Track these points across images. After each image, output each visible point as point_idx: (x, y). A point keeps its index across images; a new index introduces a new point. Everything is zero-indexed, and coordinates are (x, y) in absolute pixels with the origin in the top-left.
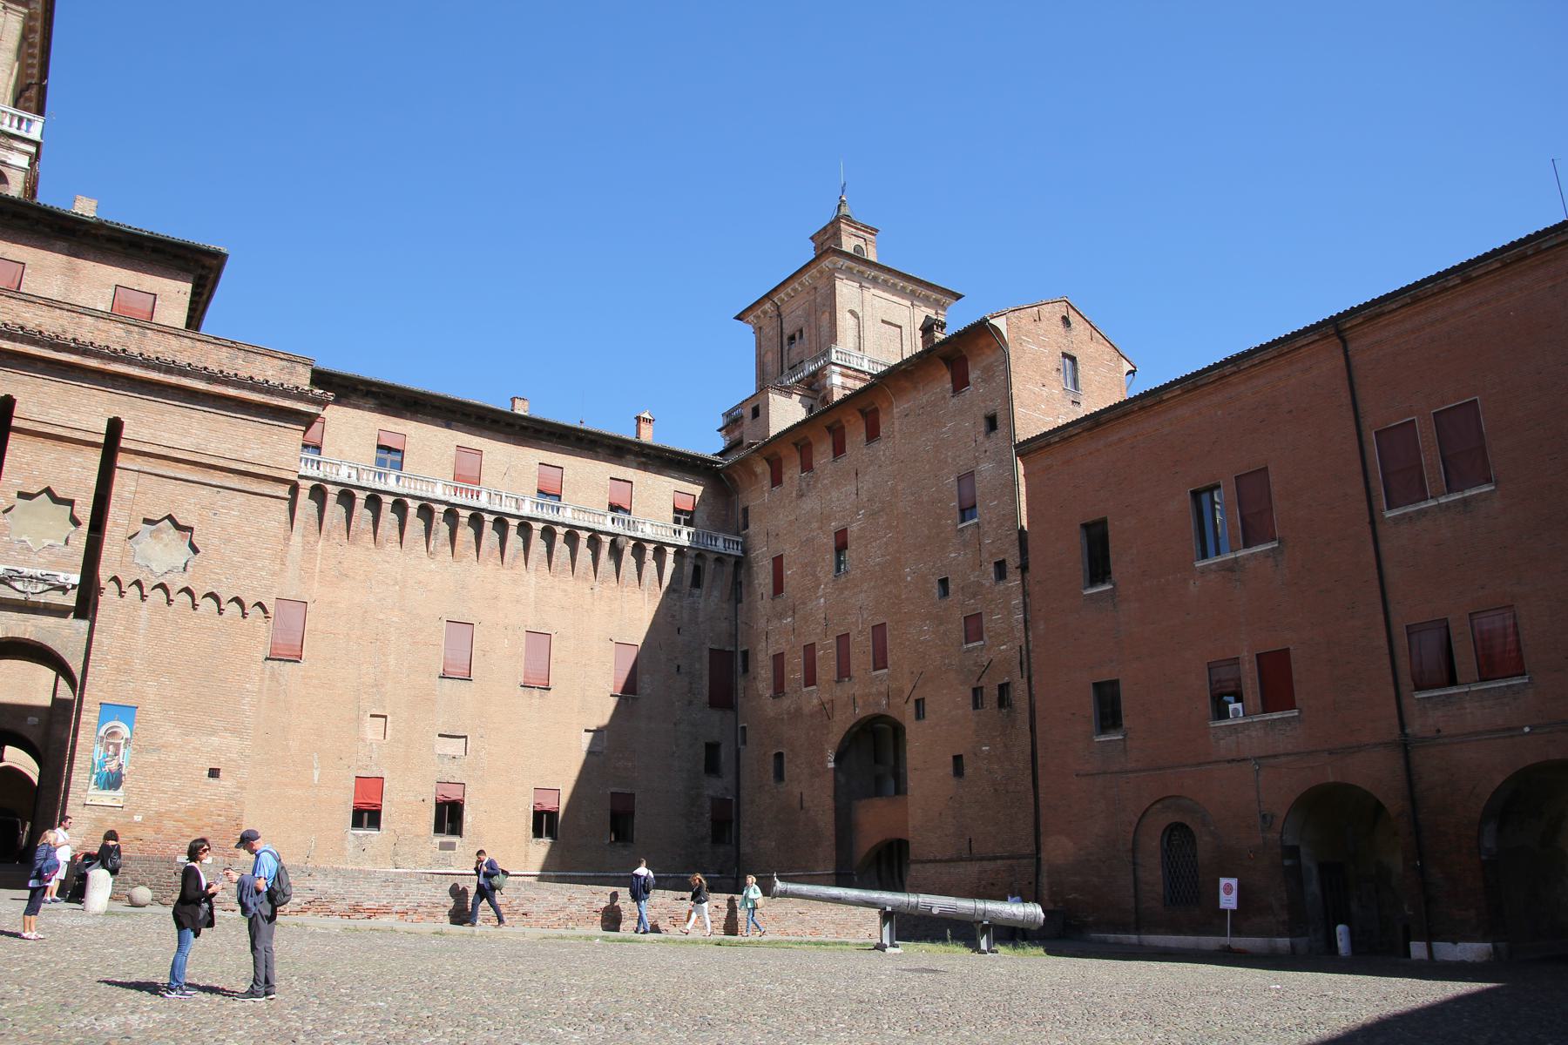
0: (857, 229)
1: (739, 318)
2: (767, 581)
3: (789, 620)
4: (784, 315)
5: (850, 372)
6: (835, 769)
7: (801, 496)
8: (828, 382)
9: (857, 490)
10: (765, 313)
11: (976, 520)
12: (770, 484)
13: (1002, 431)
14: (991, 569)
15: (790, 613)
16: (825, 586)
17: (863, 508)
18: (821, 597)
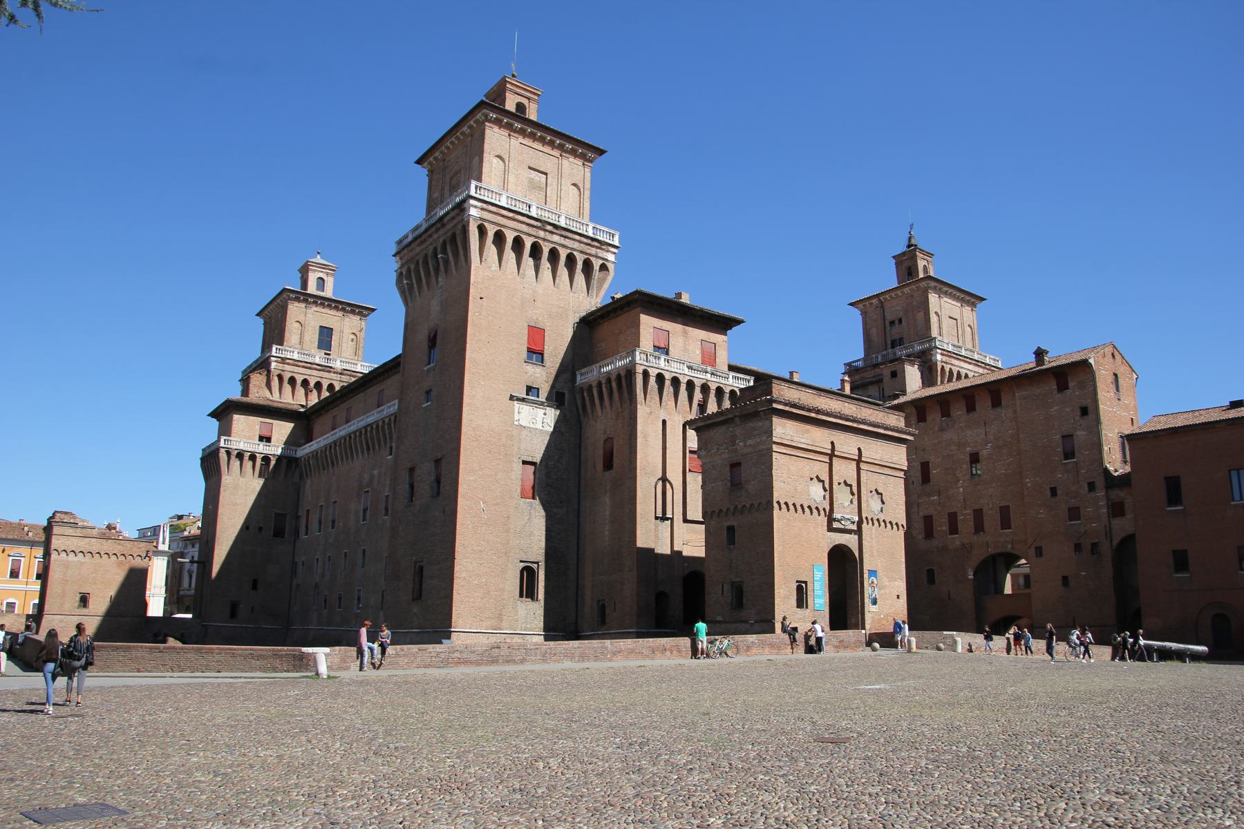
0: (923, 254)
1: (851, 304)
2: (917, 475)
3: (936, 497)
4: (885, 307)
5: (945, 352)
6: (974, 580)
7: (942, 430)
8: (933, 358)
9: (986, 432)
10: (871, 304)
11: (1075, 460)
12: (916, 421)
13: (1091, 416)
14: (1086, 485)
15: (936, 494)
16: (964, 481)
17: (990, 443)
18: (961, 487)
